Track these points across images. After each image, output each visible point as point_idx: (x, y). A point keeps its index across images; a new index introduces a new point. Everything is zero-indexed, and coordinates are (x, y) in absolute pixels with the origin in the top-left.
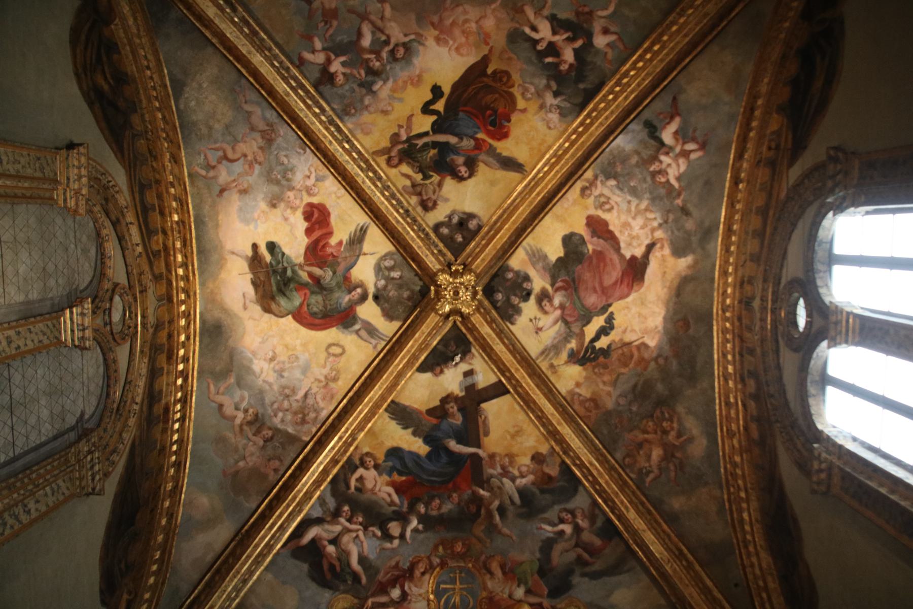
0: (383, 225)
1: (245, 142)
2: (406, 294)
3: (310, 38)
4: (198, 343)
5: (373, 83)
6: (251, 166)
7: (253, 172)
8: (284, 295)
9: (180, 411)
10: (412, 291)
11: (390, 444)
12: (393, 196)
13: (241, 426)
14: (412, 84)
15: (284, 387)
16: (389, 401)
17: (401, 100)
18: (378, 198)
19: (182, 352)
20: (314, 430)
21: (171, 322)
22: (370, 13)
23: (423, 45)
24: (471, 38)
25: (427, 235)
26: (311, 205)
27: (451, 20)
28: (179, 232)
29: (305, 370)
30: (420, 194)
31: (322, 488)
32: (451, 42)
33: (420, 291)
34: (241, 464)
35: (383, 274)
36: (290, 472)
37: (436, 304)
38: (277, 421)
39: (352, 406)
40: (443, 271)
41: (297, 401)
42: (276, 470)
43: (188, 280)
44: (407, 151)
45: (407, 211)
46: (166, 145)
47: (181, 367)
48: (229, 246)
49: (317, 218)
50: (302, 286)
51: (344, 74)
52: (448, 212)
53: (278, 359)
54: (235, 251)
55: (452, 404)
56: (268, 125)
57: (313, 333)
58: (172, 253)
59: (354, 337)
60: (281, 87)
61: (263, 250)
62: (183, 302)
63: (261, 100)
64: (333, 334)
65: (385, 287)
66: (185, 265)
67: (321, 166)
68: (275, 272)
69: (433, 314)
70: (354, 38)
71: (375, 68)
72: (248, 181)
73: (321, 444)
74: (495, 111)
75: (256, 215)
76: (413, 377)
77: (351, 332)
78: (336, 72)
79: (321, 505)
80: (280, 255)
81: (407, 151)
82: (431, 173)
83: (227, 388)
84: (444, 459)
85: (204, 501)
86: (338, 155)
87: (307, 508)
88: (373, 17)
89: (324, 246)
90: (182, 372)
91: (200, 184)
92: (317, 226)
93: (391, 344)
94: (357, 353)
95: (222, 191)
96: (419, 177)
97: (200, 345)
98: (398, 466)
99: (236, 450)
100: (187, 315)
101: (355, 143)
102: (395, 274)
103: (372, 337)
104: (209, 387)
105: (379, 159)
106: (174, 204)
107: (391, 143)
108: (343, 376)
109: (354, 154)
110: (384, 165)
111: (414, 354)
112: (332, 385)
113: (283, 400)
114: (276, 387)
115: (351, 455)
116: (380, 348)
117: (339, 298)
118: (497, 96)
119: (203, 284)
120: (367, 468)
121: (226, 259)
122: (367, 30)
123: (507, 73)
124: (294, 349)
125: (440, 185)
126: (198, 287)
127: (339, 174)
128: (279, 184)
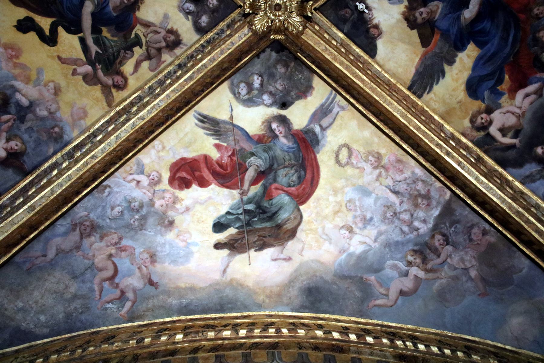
0: (197, 95)
1: (94, 255)
2: (281, 69)
4: (327, 316)
5: (18, 105)
6: (123, 249)
7: (131, 247)
8: (276, 213)
9: (404, 342)
10: (278, 62)
11: (461, 94)
12: (161, 83)
13: (427, 271)
14: (17, 57)
15: (384, 218)
16: (408, 93)
17: (40, 71)
18: (162, 101)
19: (336, 335)
20: (438, 184)
21: (300, 346)
25: (208, 42)
26: (171, 181)
28: (197, 333)
29: (365, 192)
30: (159, 50)
31: (511, 178)
33: (277, 52)
34: (473, 273)
35: (256, 96)
36: (486, 216)
37: (291, 33)
38: (424, 229)
39: (410, 138)
40: (251, 24)
41: (401, 203)
42: (485, 233)
43: (253, 324)
44: (105, 66)
45: (180, 66)
46: (91, 349)
47: (353, 337)
48: (216, 276)
49: (187, 173)
50: (267, 193)
51: (8, 140)
52: (181, 15)
53: (351, 224)
54: (223, 268)
55: (417, 14)
56: (74, 230)
57: (322, 181)
58: (220, 342)
59: (329, 132)
60: (22, 215)
61: (222, 237)
62: (278, 331)
63: (43, 237)
64: (324, 158)
65: (271, 93)
66: (235, 327)
67: (126, 167)
68: (248, 224)
69: (303, 37)
72: (141, 253)
73: (454, 177)
75: (182, 244)
76: (381, 63)
77: (323, 134)
78: (6, 149)
79: (534, 181)
80: (230, 217)
81: (105, 66)
82: (133, 35)
83: (381, 286)
84: (487, 25)
85: (516, 323)
86: (109, 149)
87: (535, 198)
89: (221, 165)
90: (358, 336)
91: (142, 307)
92: (197, 174)
93: (339, 89)
94: (348, 132)
95: (151, 283)
96: (138, 51)
97: (329, 313)
98: (491, 83)
99: (456, 278)
100: (293, 327)
101: (96, 127)
102: (257, 82)
103: (331, 111)
104: (379, 306)
105: (117, 100)
106: (164, 338)
107: (95, 84)
108: (376, 148)
109: (110, 129)
110: (124, 94)
111: (351, 62)
112: (385, 161)
113: (399, 219)
114: (383, 228)
115: (472, 141)
116: (344, 103)
117: (282, 150)
119: (260, 307)
120: (491, 123)
121: (232, 280)
124: (339, 204)
125: (147, 25)
126: (262, 313)
127: (135, 147)
128: (144, 217)
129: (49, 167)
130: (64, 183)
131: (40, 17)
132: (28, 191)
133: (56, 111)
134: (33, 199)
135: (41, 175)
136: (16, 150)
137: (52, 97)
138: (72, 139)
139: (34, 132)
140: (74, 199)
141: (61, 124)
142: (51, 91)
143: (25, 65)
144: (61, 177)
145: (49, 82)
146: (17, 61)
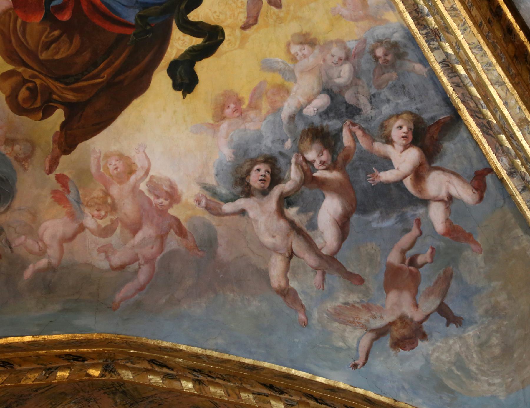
3: (453, 231)
5: (326, 113)
14: (239, 101)
17: (267, 66)
22: (316, 269)
23: (206, 187)
24: (97, 193)
27: (140, 235)
32: (143, 187)
51: (389, 141)
70: (355, 217)
71: (317, 146)
74: (50, 18)
78: (406, 147)
88: (310, 259)
118: (44, 56)
122: (327, 235)
123: (17, 108)
129: (450, 78)
130: (485, 60)
131: (169, 50)
132: (489, 122)
133: (345, 48)
134: (507, 120)
135: (463, 94)
136: (409, 129)
137: (317, 51)
138: (402, 27)
139: (379, 94)
140: (520, 40)
141: (371, 42)
142: (306, 52)
143: (255, 90)
144: (472, 63)
145: (288, 51)
146: (247, 102)
